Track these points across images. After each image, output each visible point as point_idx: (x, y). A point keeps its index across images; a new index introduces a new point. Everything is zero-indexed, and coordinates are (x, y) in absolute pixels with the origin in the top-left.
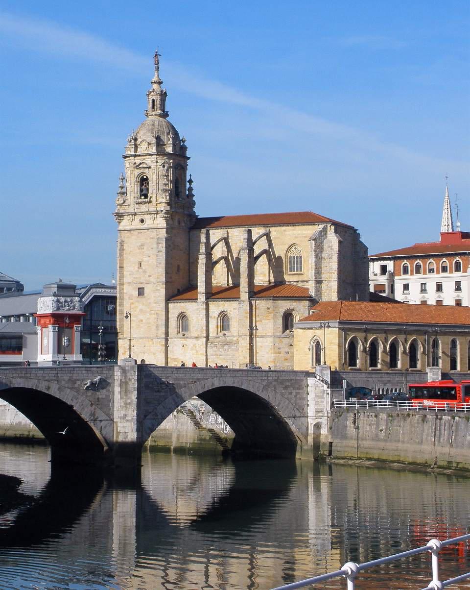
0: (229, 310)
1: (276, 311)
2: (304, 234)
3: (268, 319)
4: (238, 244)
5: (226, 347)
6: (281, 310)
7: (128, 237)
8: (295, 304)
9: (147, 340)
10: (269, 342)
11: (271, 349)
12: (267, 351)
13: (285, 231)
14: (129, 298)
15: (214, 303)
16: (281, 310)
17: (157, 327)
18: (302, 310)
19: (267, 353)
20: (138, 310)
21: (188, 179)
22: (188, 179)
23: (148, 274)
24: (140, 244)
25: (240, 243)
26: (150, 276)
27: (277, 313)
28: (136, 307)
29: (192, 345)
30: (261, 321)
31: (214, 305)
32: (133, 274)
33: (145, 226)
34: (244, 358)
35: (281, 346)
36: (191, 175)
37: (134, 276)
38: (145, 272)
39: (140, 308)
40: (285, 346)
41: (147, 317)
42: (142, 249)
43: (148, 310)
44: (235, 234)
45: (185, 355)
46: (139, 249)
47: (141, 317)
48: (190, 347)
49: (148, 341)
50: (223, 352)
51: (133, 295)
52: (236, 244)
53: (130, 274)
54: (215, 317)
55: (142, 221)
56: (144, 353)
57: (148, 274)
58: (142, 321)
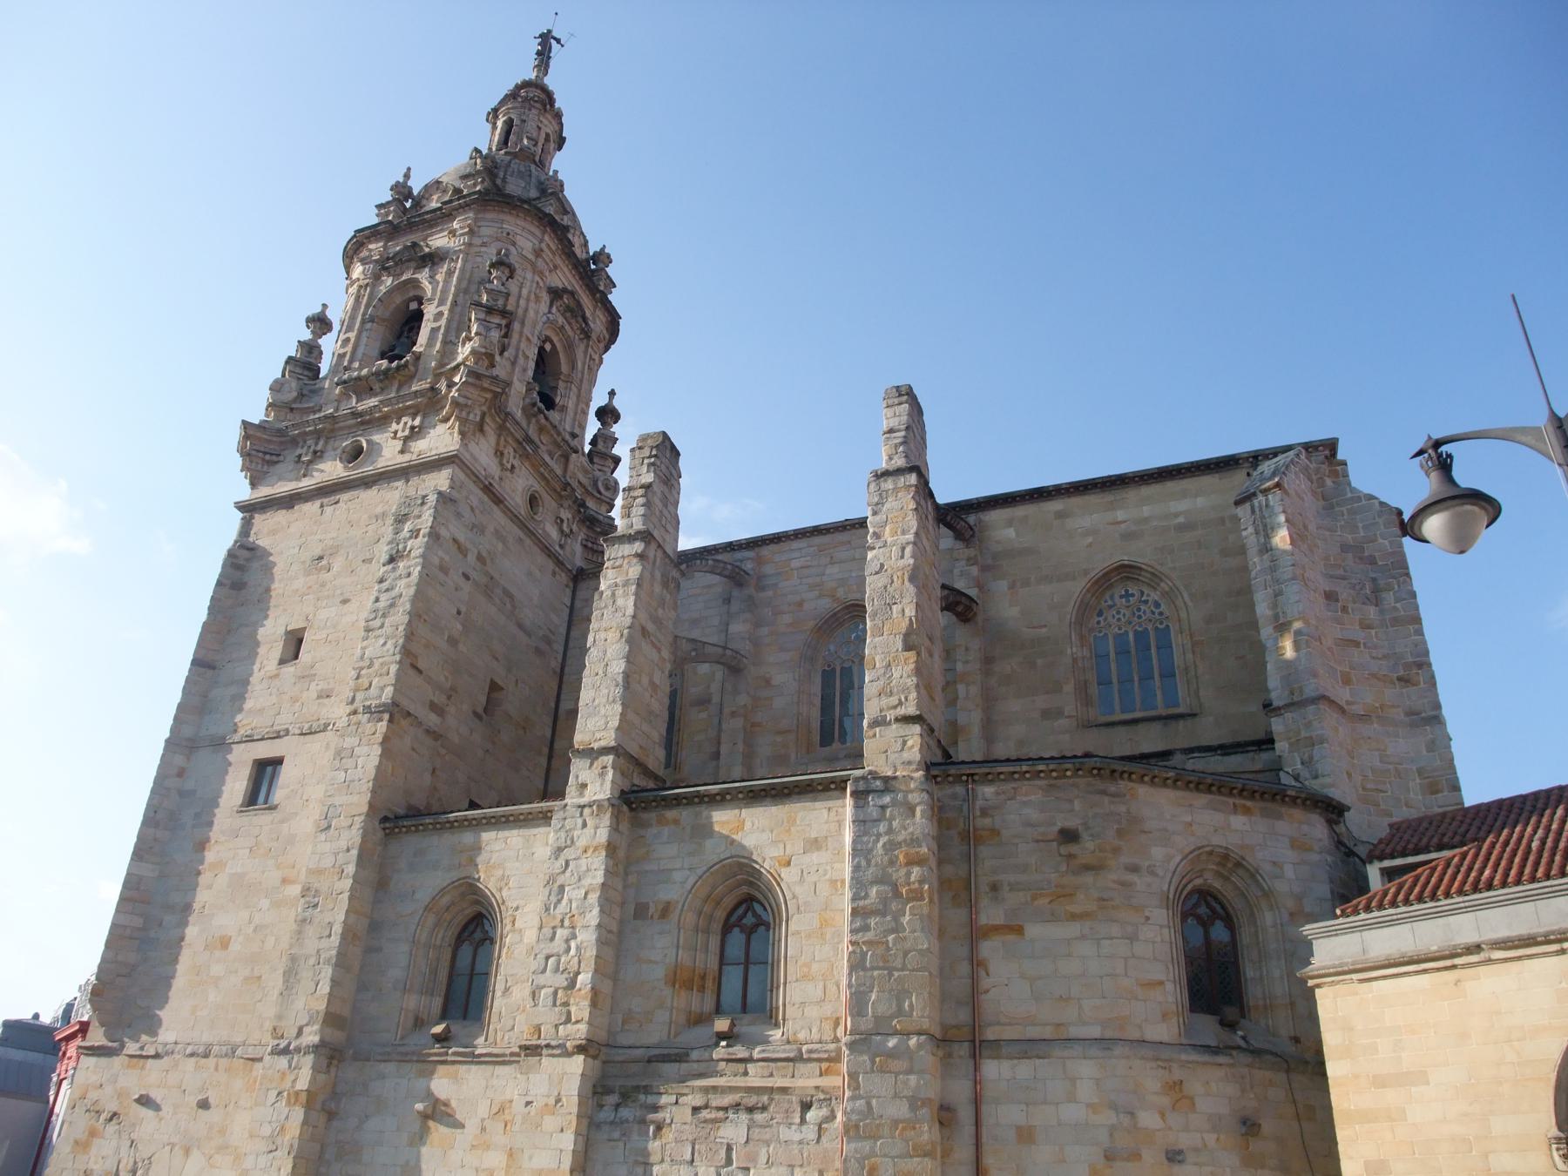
1: (1125, 859)
2: (1176, 515)
3: (1074, 917)
4: (806, 606)
5: (734, 1130)
6: (1157, 853)
7: (273, 532)
8: (1238, 821)
9: (224, 1062)
10: (1086, 1091)
11: (1109, 1157)
13: (1060, 515)
15: (671, 814)
16: (1157, 853)
17: (291, 975)
18: (1289, 871)
21: (598, 399)
22: (598, 399)
23: (314, 688)
24: (318, 552)
25: (821, 596)
26: (325, 695)
27: (1134, 869)
29: (483, 1110)
30: (1019, 930)
31: (666, 831)
33: (367, 469)
35: (1184, 1141)
36: (612, 393)
38: (307, 677)
40: (1211, 1139)
44: (795, 564)
46: (308, 573)
52: (800, 604)
54: (665, 911)
56: (187, 1152)
57: (314, 688)
58: (225, 943)
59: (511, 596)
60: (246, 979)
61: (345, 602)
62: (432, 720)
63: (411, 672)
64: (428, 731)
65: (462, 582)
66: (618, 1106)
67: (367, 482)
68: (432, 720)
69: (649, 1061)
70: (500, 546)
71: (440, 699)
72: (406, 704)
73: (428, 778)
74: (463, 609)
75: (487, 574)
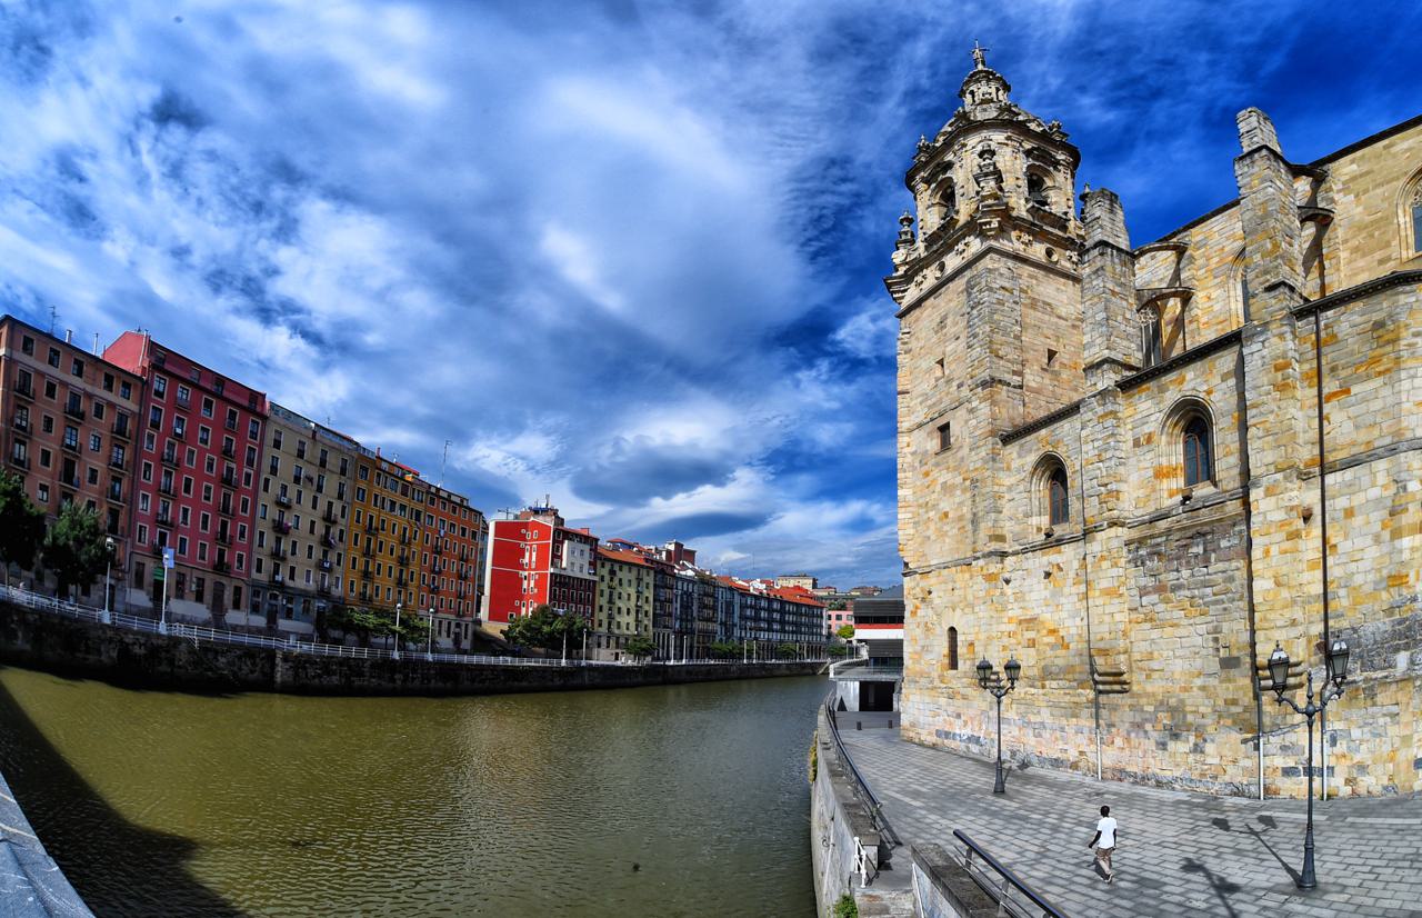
0: (1205, 388)
9: (959, 568)
12: (1377, 527)
14: (921, 462)
19: (1377, 540)
20: (938, 488)
23: (955, 384)
28: (934, 480)
32: (926, 399)
33: (949, 270)
34: (1278, 584)
37: (929, 402)
39: (941, 480)
41: (957, 500)
42: (942, 328)
43: (959, 479)
45: (1057, 606)
46: (936, 332)
47: (945, 506)
48: (1072, 575)
49: (961, 571)
50: (1185, 573)
51: (927, 451)
53: (921, 403)
55: (942, 267)
57: (955, 384)
58: (946, 515)
59: (1049, 304)
60: (959, 529)
61: (957, 339)
62: (1016, 380)
63: (995, 360)
64: (1015, 387)
65: (1014, 306)
66: (1138, 548)
67: (951, 278)
68: (1016, 380)
69: (1151, 522)
70: (1034, 282)
71: (1016, 367)
72: (997, 375)
73: (1021, 409)
74: (1019, 319)
75: (1030, 297)
